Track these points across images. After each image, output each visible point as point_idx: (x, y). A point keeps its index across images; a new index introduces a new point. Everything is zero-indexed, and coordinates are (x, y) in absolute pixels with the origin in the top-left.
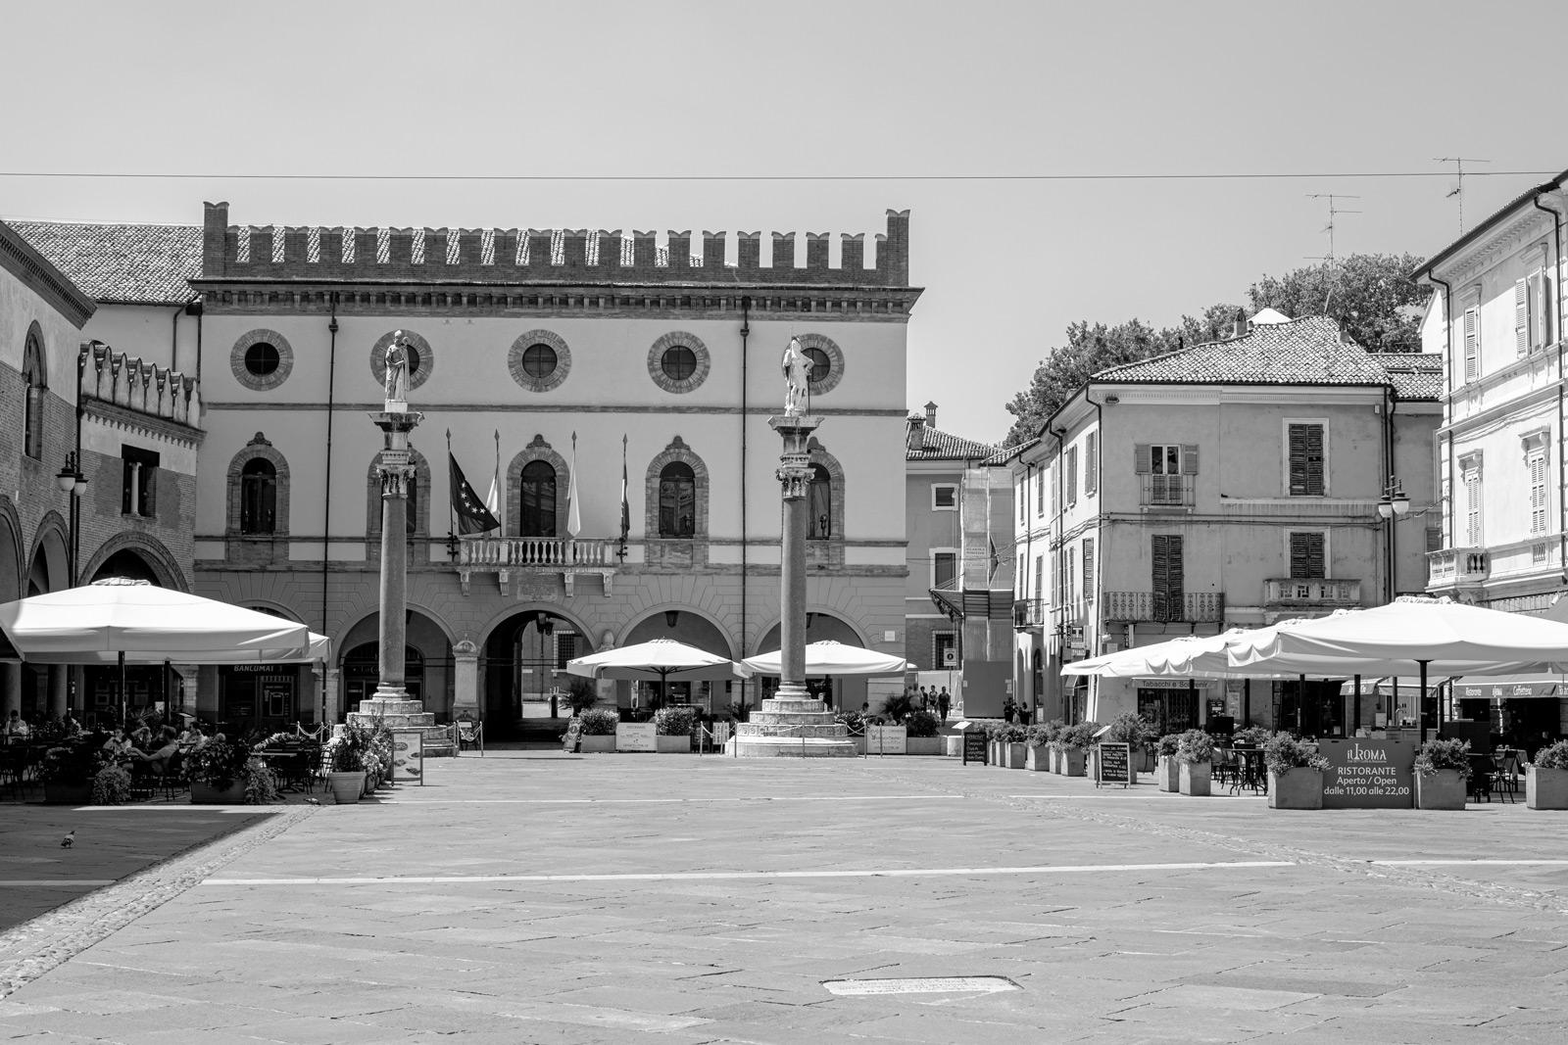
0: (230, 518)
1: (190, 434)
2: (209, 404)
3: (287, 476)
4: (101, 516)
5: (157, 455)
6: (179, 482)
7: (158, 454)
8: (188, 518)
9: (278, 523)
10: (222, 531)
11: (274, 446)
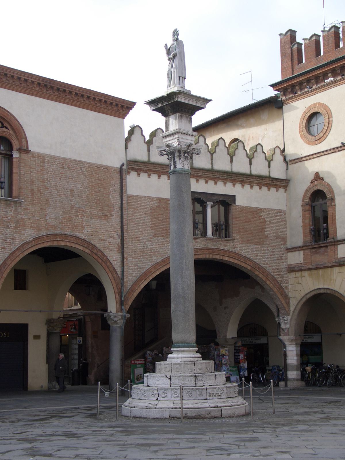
0: (305, 236)
1: (281, 184)
2: (290, 161)
3: (333, 199)
4: (160, 239)
5: (233, 197)
6: (263, 214)
7: (234, 196)
8: (277, 237)
9: (330, 231)
10: (300, 243)
11: (326, 180)
